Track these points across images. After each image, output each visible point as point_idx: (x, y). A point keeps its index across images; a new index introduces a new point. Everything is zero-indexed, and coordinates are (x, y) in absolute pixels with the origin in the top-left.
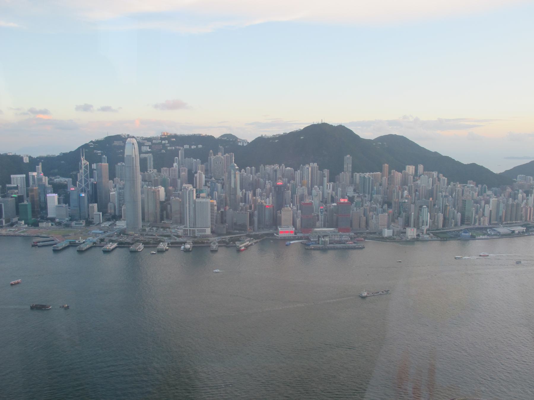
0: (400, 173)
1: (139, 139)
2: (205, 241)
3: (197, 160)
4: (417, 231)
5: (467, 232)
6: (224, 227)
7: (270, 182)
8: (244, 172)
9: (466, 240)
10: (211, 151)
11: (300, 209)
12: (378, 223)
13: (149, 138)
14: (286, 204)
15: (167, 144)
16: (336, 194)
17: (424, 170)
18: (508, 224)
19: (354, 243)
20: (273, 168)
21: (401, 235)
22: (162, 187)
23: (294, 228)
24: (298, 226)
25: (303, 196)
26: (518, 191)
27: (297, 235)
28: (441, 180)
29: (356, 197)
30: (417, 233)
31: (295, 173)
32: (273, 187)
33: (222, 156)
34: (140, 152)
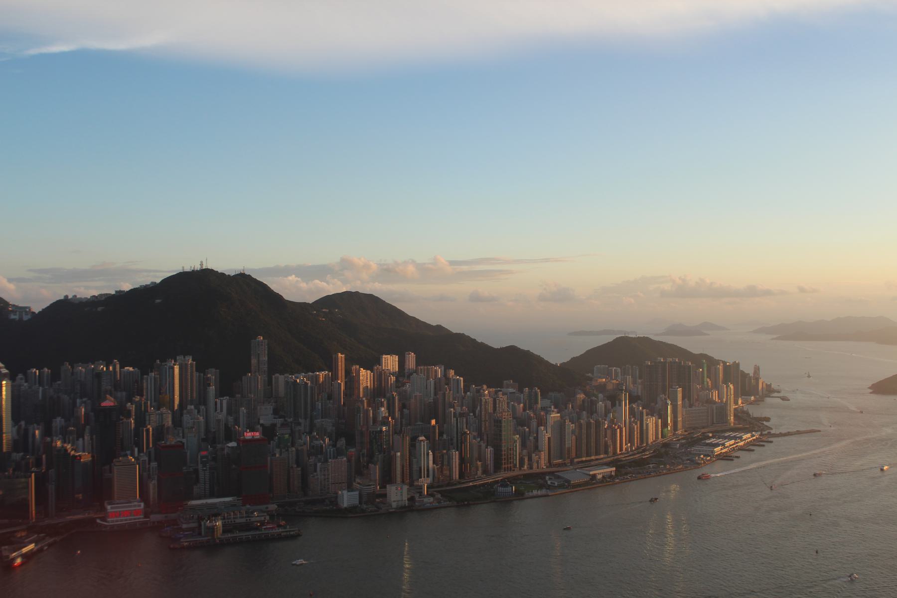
0: (369, 372)
4: (409, 490)
5: (506, 486)
7: (85, 402)
8: (24, 381)
9: (506, 502)
12: (328, 478)
16: (237, 421)
17: (418, 363)
18: (582, 462)
19: (279, 526)
21: (377, 500)
23: (142, 504)
26: (597, 397)
27: (149, 518)
28: (452, 382)
29: (279, 425)
30: (408, 494)
31: (142, 379)
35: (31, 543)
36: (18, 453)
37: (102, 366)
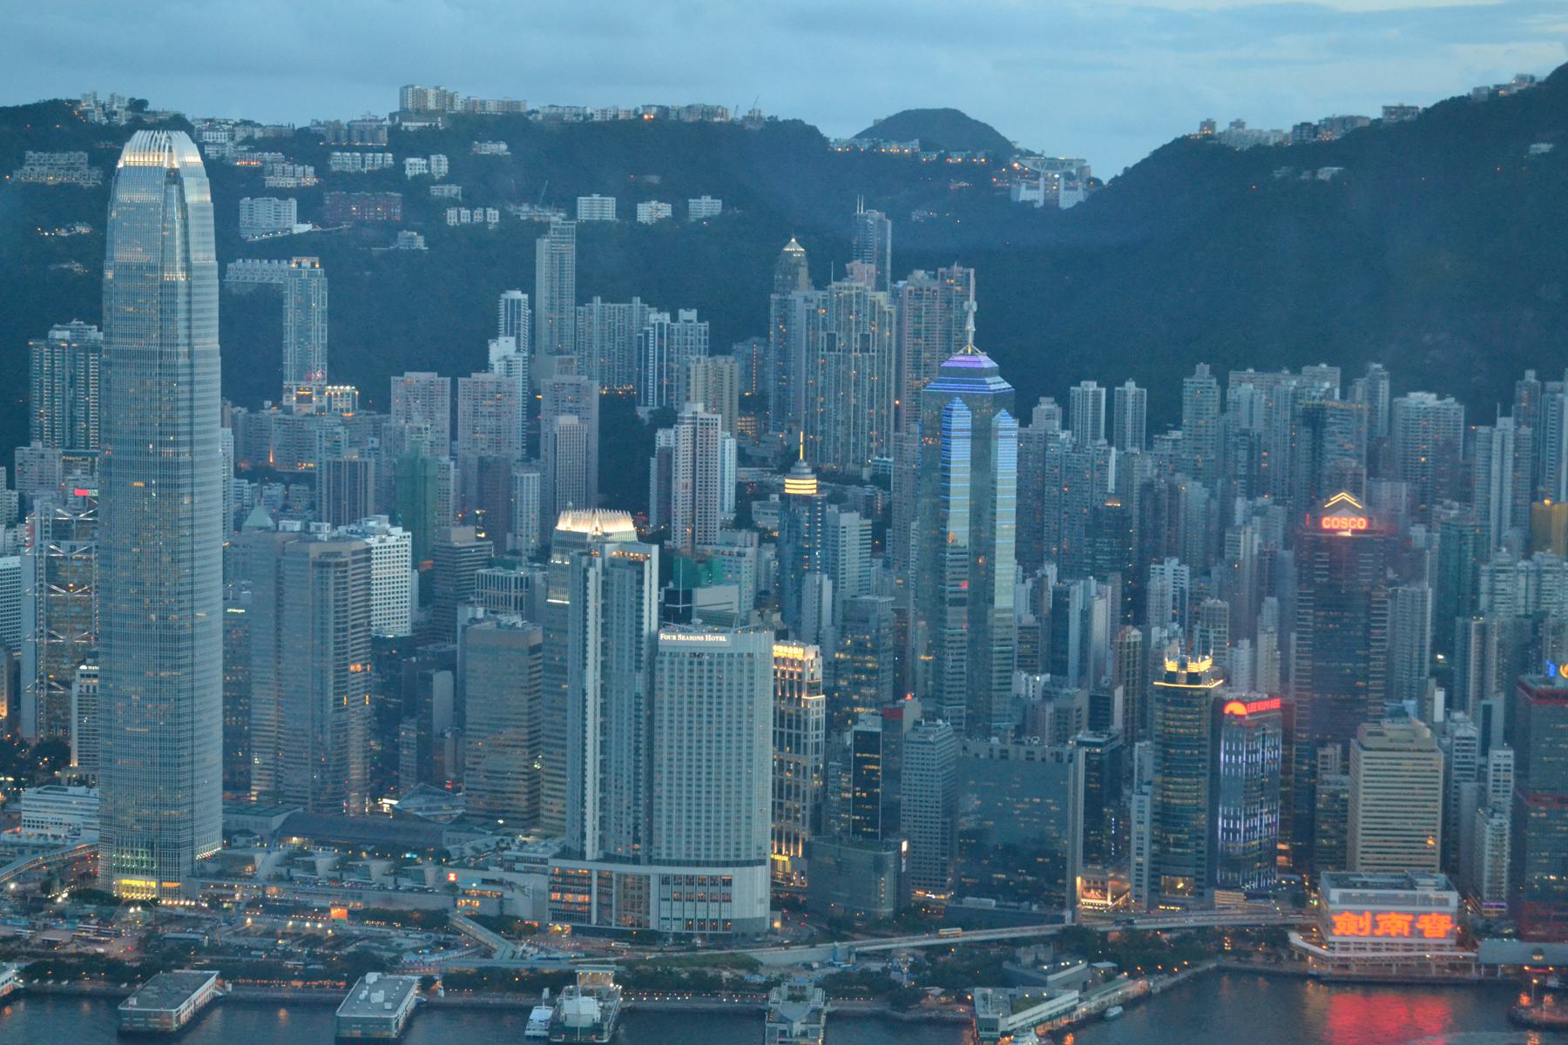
1: (222, 137)
2: (726, 974)
3: (675, 318)
6: (878, 866)
7: (1261, 512)
8: (1057, 423)
10: (794, 248)
11: (1509, 737)
13: (303, 134)
14: (1389, 693)
15: (445, 180)
20: (1295, 396)
22: (394, 523)
24: (1486, 874)
25: (1535, 630)
27: (1474, 946)
31: (1469, 436)
32: (1287, 546)
33: (881, 286)
34: (230, 244)
35: (1067, 985)
36: (1033, 671)
37: (1327, 385)
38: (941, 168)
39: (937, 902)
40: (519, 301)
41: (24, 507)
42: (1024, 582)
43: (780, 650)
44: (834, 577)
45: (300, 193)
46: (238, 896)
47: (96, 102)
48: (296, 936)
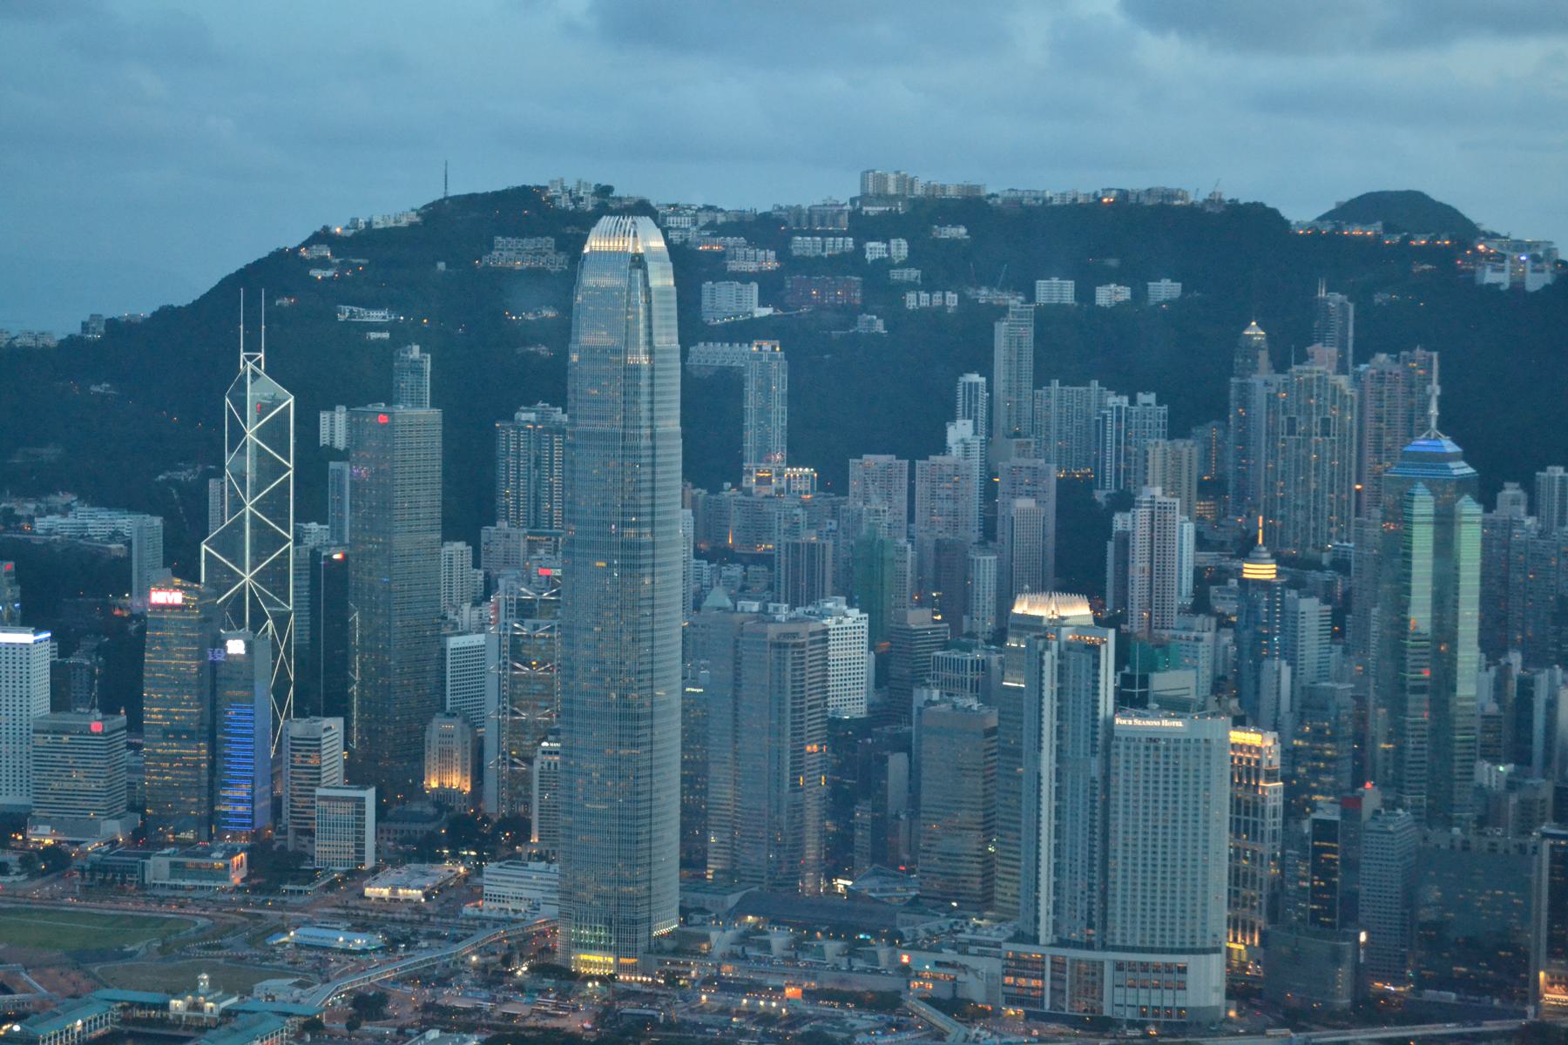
3: (1133, 401)
6: (1336, 957)
8: (1522, 509)
10: (1255, 331)
13: (765, 217)
22: (850, 604)
33: (1342, 369)
34: (692, 328)
38: (1405, 252)
39: (1396, 994)
40: (977, 384)
41: (490, 587)
42: (1487, 670)
43: (1237, 736)
44: (1292, 663)
45: (761, 277)
46: (693, 973)
47: (563, 188)
48: (751, 1014)
